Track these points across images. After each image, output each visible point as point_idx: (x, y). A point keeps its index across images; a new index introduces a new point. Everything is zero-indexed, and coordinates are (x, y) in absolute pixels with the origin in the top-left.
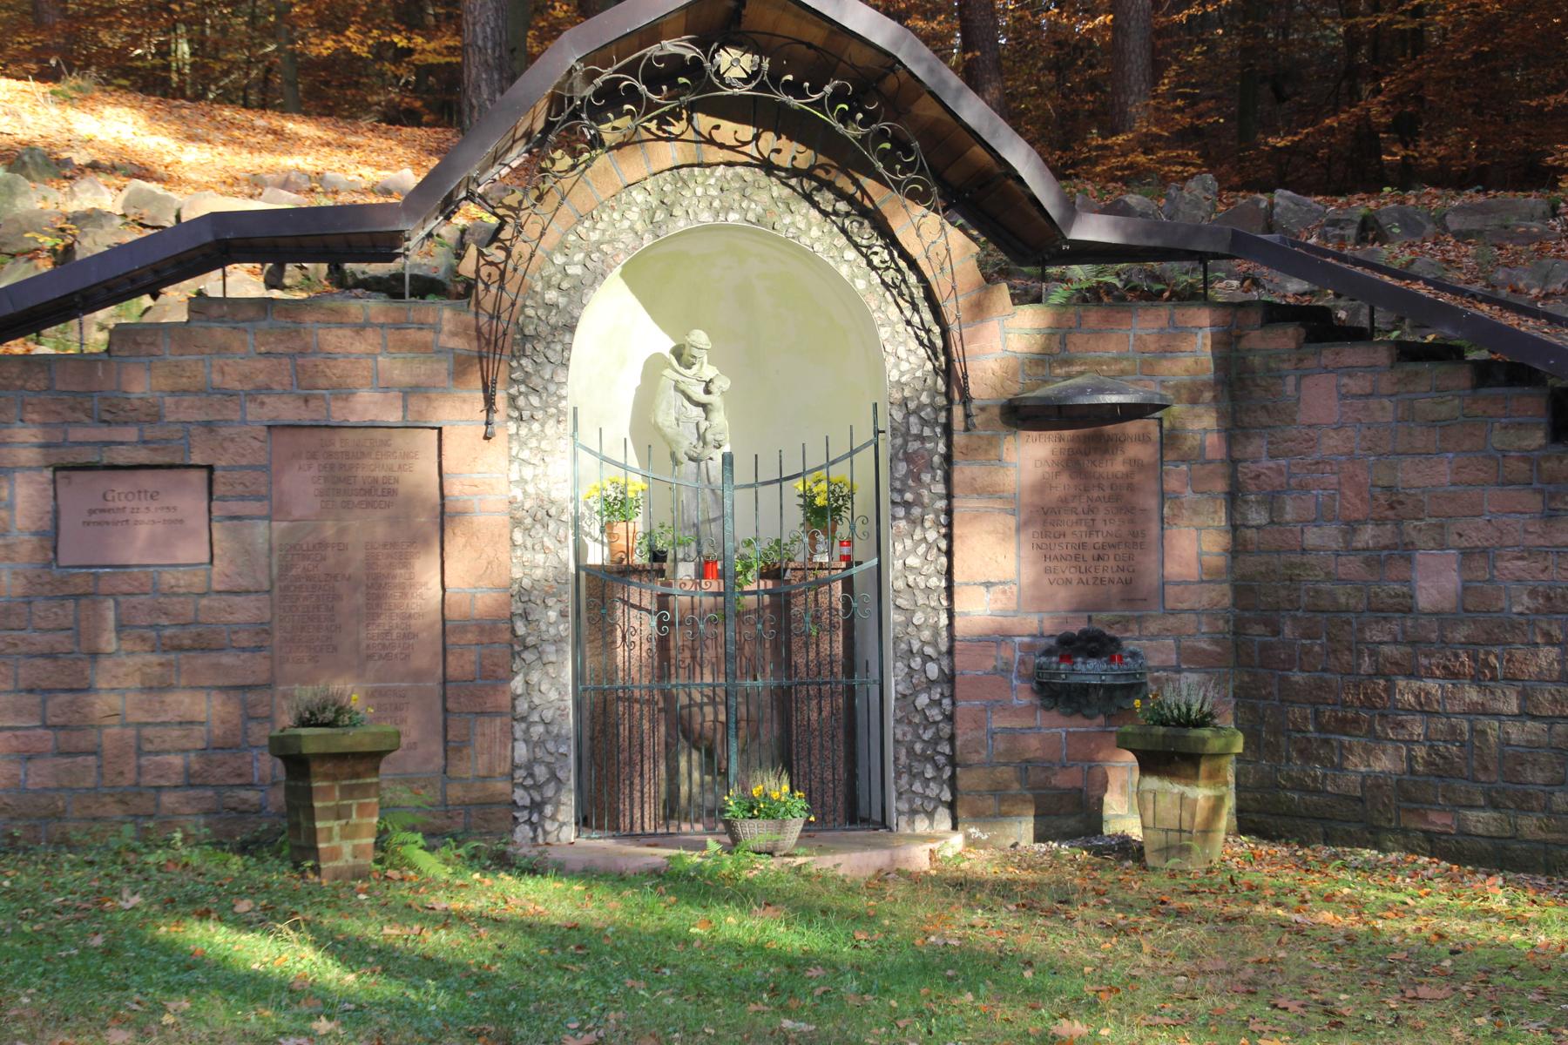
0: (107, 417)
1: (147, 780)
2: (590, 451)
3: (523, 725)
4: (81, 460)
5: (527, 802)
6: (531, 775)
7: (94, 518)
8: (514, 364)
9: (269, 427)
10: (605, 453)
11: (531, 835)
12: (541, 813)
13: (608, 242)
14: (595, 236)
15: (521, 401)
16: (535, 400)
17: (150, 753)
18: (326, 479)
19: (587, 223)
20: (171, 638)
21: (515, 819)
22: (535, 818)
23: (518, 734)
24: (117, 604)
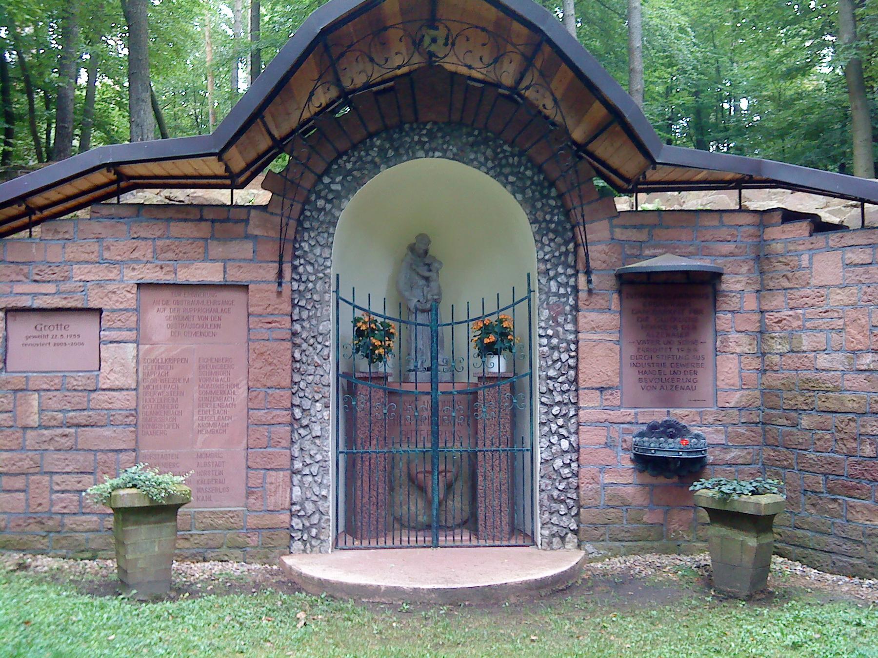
0: (38, 278)
1: (56, 508)
2: (347, 302)
3: (299, 477)
4: (21, 304)
5: (300, 526)
6: (304, 509)
7: (30, 341)
8: (297, 246)
9: (139, 285)
10: (356, 303)
11: (302, 547)
12: (309, 533)
13: (358, 170)
14: (349, 166)
15: (301, 269)
16: (309, 268)
17: (58, 492)
18: (175, 318)
19: (345, 158)
20: (71, 418)
21: (292, 537)
22: (305, 537)
23: (296, 482)
24: (40, 397)
